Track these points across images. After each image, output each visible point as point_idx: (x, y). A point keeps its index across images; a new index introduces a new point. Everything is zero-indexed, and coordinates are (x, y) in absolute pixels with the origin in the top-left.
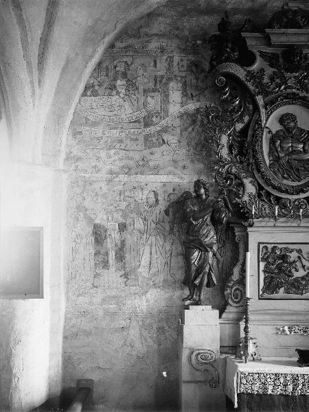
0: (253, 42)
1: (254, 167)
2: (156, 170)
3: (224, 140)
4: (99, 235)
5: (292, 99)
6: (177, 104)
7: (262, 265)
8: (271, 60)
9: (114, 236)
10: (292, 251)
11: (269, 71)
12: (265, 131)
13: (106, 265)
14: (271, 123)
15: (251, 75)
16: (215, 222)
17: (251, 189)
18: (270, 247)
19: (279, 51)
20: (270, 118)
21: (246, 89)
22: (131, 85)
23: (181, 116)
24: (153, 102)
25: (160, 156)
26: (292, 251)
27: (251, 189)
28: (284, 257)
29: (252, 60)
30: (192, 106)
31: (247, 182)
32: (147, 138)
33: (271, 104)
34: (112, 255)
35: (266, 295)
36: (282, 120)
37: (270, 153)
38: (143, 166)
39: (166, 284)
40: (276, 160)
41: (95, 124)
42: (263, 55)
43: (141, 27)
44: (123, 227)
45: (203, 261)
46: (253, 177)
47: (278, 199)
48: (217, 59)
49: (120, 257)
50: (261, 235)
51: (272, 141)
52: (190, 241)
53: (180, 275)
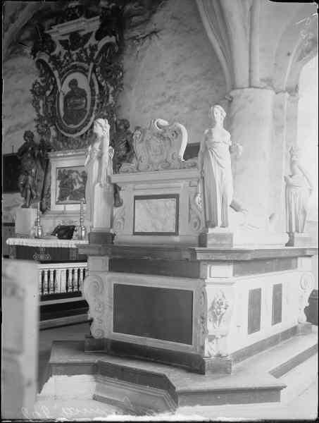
5: (75, 68)
7: (59, 182)
8: (63, 43)
10: (72, 172)
12: (61, 94)
14: (65, 89)
17: (54, 133)
18: (62, 170)
19: (67, 38)
20: (65, 82)
21: (49, 68)
26: (72, 172)
27: (54, 133)
28: (67, 177)
35: (60, 202)
37: (65, 109)
42: (61, 42)
43: (19, 36)
46: (55, 125)
47: (67, 137)
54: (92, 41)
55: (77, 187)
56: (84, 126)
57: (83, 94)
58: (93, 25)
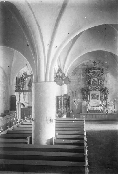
0: (90, 71)
1: (90, 85)
2: (79, 85)
3: (87, 82)
4: (73, 93)
5: (95, 77)
6: (82, 77)
8: (92, 72)
9: (75, 93)
11: (92, 74)
13: (74, 96)
14: (92, 80)
15: (90, 74)
16: (86, 92)
17: (90, 87)
22: (76, 74)
23: (83, 78)
24: (79, 77)
25: (80, 83)
27: (90, 87)
29: (90, 73)
30: (83, 77)
31: (90, 87)
32: (78, 81)
33: (92, 78)
34: (75, 95)
36: (93, 79)
38: (78, 84)
39: (81, 99)
40: (93, 84)
41: (72, 79)
44: (76, 92)
45: (85, 96)
48: (86, 73)
49: (75, 95)
50: (91, 93)
51: (92, 82)
52: (83, 94)
53: (82, 97)
54: (98, 73)
55: (96, 97)
56: (96, 87)
57: (96, 81)
58: (99, 71)
